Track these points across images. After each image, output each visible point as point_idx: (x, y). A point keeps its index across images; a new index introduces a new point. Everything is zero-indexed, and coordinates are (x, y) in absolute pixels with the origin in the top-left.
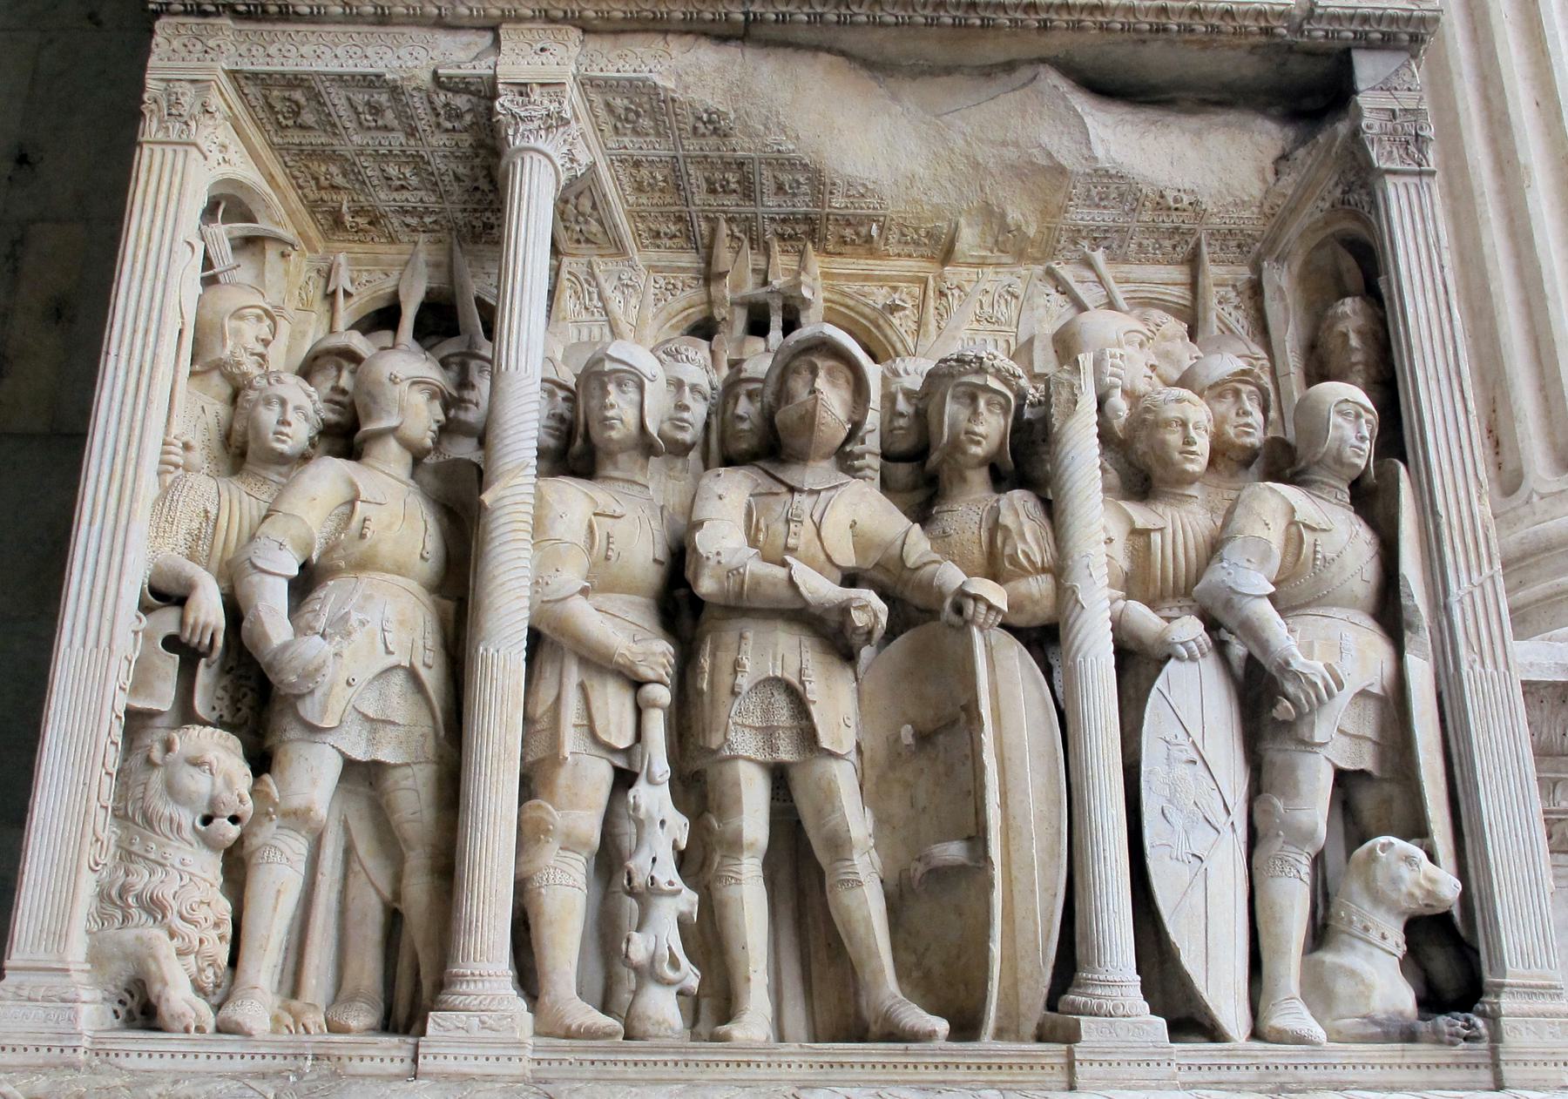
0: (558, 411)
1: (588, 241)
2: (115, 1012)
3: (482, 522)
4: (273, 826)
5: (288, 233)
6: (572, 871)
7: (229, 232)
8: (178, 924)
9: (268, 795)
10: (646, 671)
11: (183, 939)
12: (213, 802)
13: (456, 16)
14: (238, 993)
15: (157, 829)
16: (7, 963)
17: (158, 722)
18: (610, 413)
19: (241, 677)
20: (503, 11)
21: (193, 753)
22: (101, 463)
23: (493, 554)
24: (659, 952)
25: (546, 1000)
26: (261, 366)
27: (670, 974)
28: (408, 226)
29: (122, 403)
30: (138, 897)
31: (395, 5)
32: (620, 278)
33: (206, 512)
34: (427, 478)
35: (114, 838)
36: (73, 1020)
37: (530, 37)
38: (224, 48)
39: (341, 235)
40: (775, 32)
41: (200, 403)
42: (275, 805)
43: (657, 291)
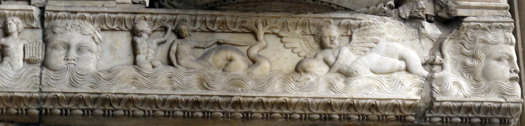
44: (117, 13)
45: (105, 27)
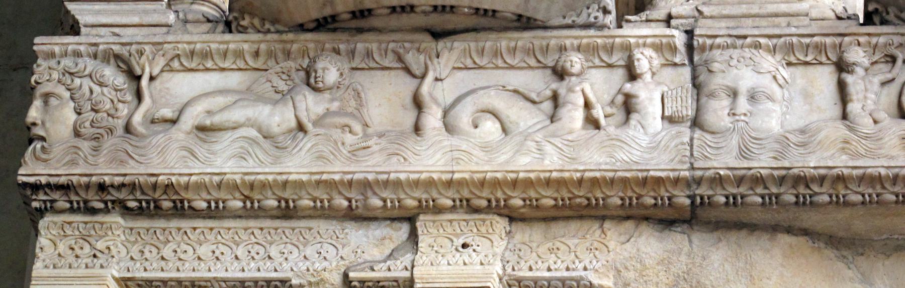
13: (366, 207)
20: (420, 201)
31: (300, 198)
37: (450, 230)
38: (114, 251)
40: (730, 214)
44: (812, 36)
45: (793, 59)
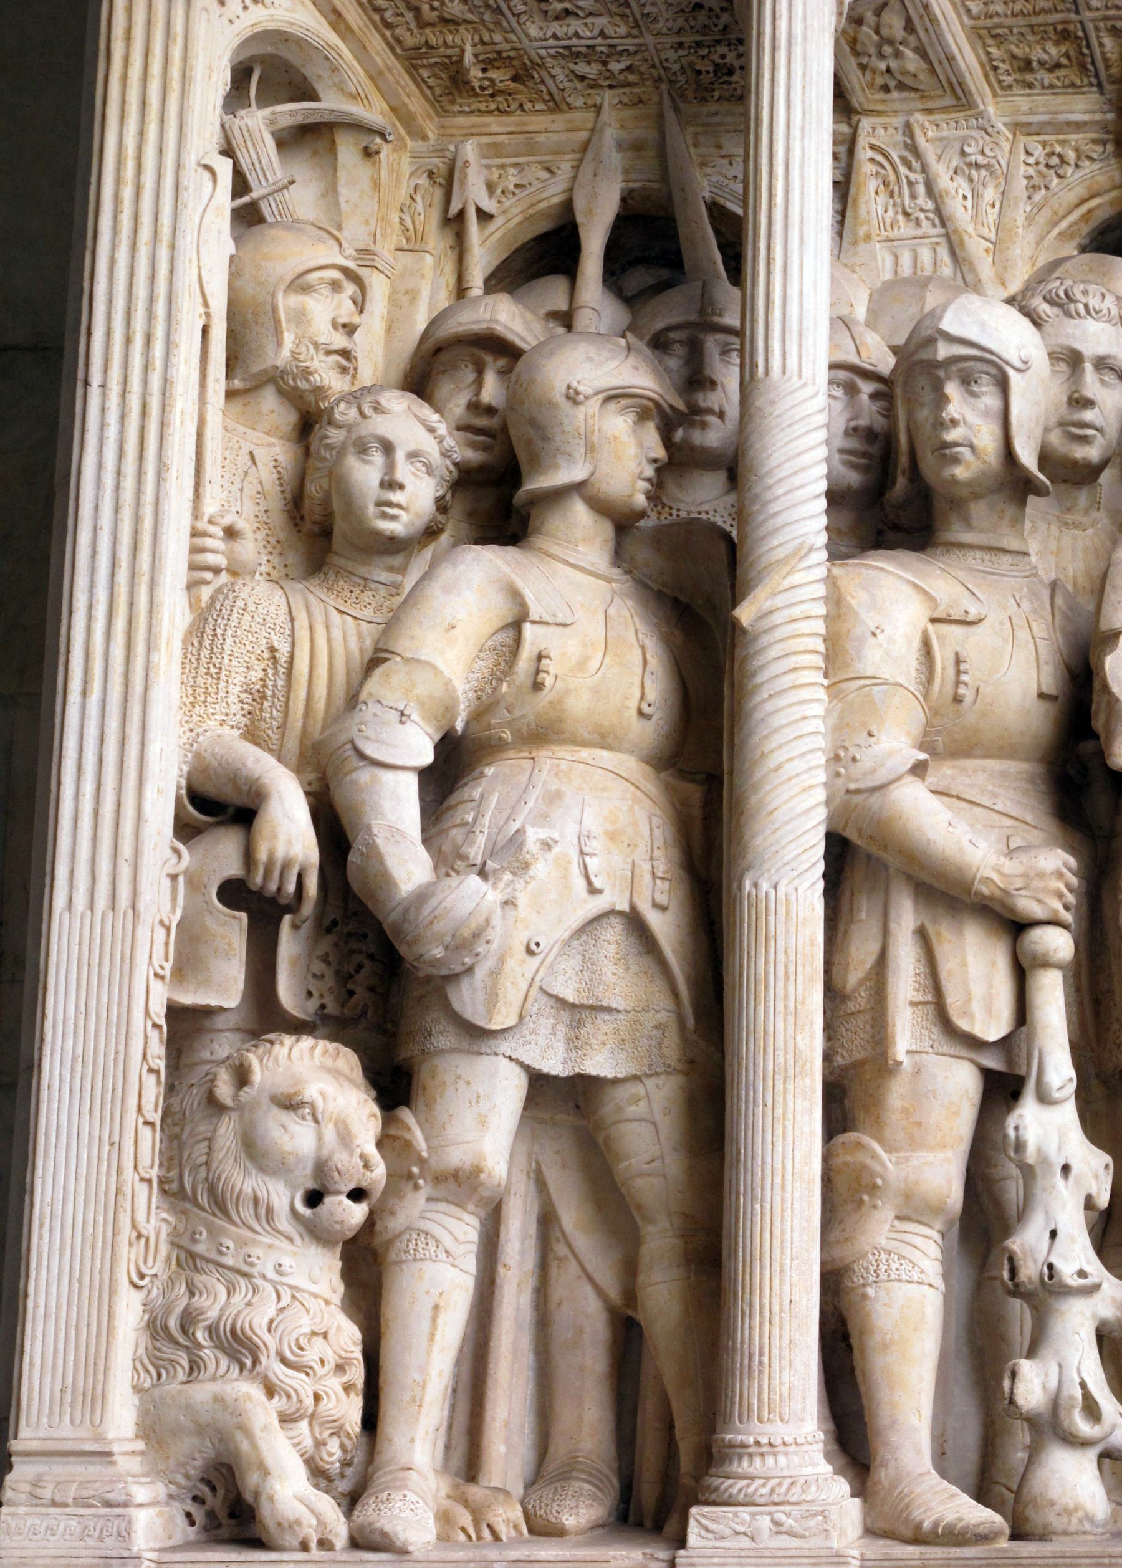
0: (863, 422)
1: (902, 86)
2: (188, 1515)
3: (739, 653)
4: (420, 1198)
5: (374, 113)
6: (916, 1255)
7: (271, 122)
8: (277, 1370)
9: (408, 1145)
10: (1028, 906)
11: (289, 1396)
12: (321, 1168)
14: (381, 1478)
15: (235, 1217)
16: (15, 1445)
17: (220, 1022)
18: (952, 435)
19: (350, 935)
21: (284, 1087)
22: (92, 585)
23: (758, 715)
24: (1065, 1393)
25: (882, 1476)
26: (344, 370)
27: (1084, 1427)
28: (582, 78)
29: (119, 473)
30: (212, 1330)
32: (963, 153)
33: (272, 650)
34: (642, 553)
35: (165, 1230)
36: (125, 1535)
39: (465, 103)
41: (247, 447)
42: (422, 1161)
43: (1031, 171)
